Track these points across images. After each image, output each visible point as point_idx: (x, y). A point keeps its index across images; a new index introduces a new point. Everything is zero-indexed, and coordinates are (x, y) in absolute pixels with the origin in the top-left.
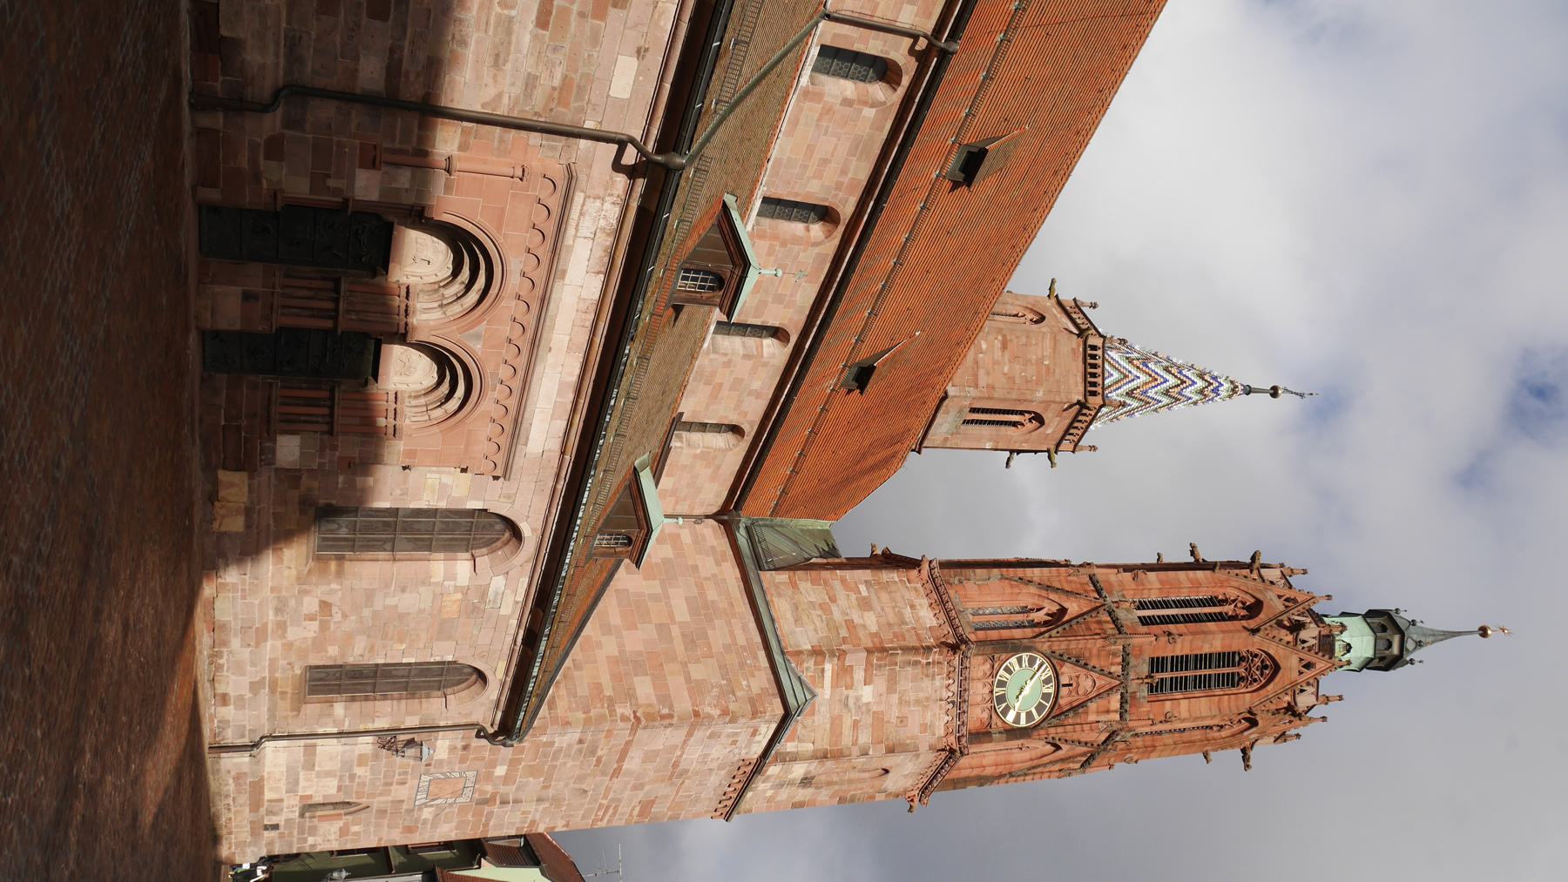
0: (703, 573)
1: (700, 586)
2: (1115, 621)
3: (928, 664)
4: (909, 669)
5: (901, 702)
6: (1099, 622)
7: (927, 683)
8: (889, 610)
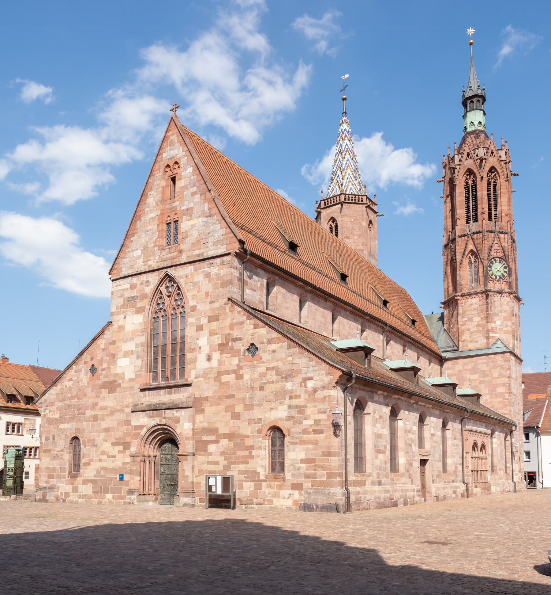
0: (461, 368)
1: (466, 370)
2: (477, 233)
3: (491, 303)
4: (492, 309)
5: (501, 312)
6: (477, 239)
7: (496, 303)
8: (473, 313)
